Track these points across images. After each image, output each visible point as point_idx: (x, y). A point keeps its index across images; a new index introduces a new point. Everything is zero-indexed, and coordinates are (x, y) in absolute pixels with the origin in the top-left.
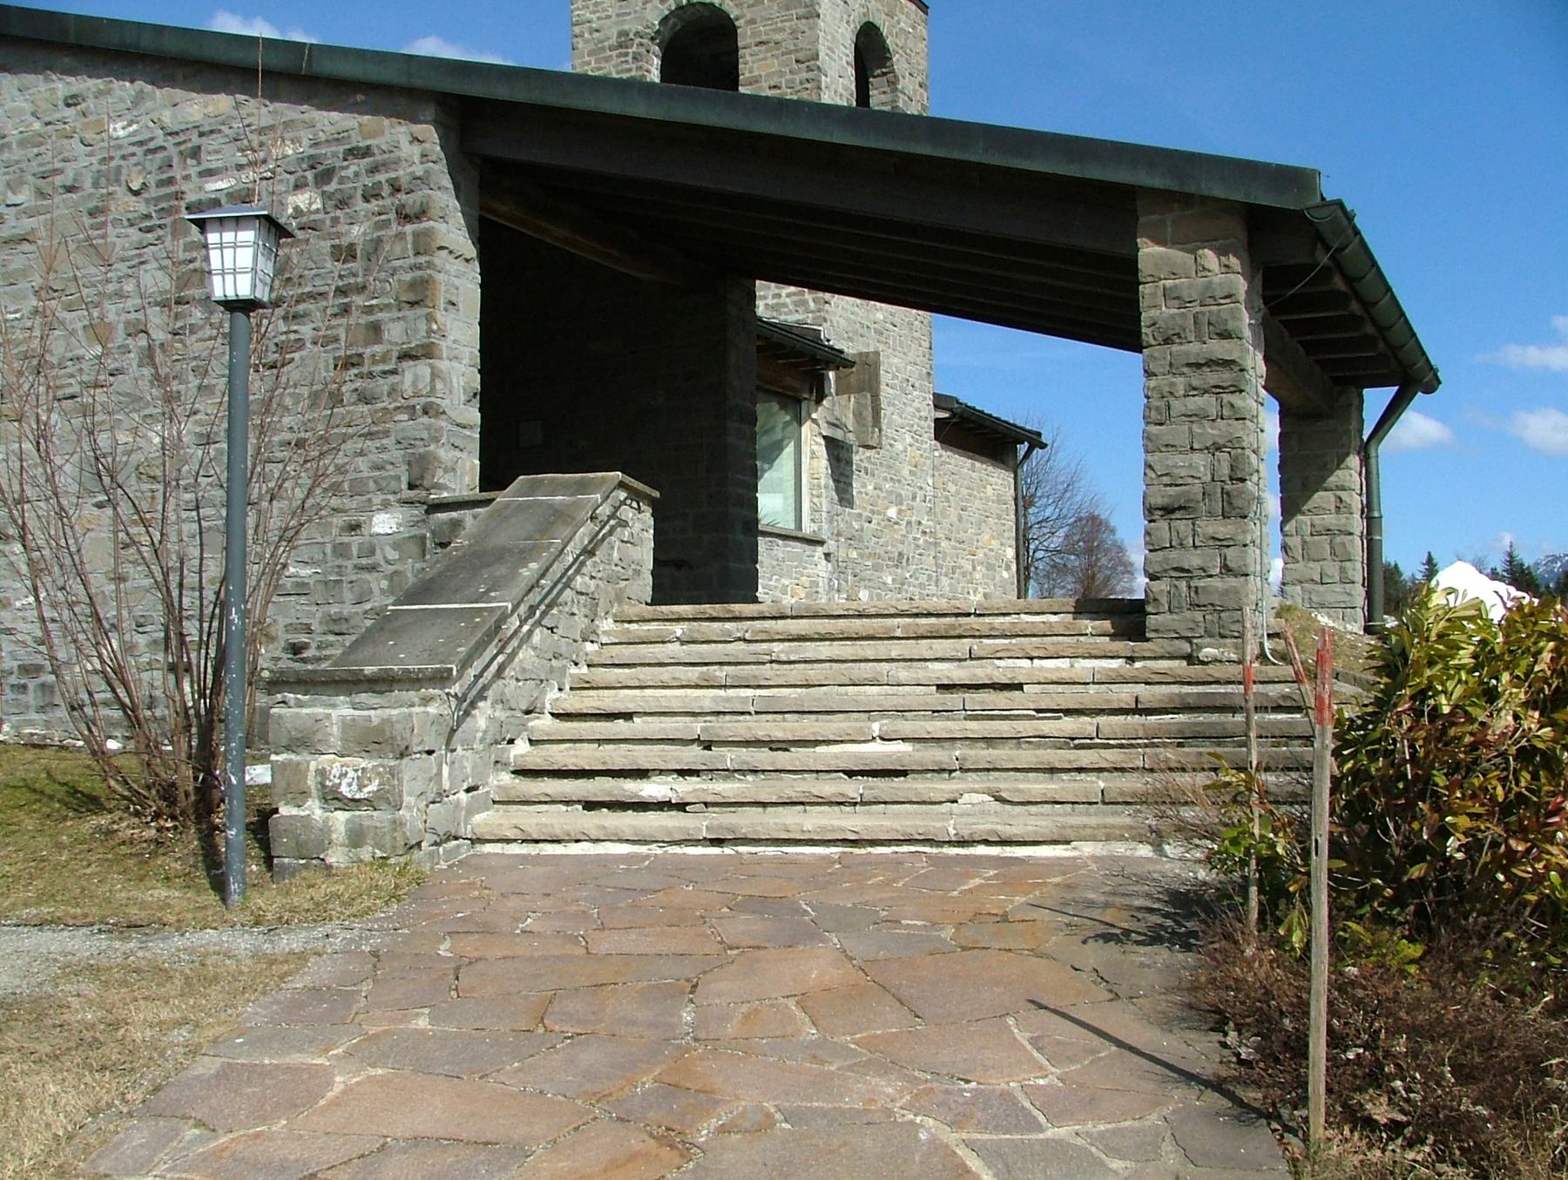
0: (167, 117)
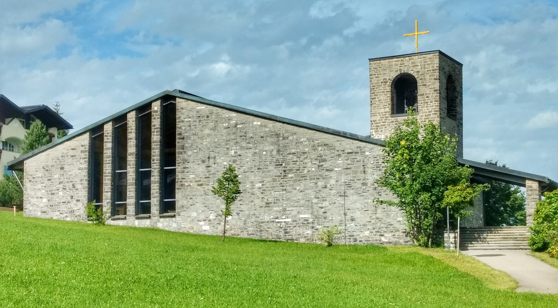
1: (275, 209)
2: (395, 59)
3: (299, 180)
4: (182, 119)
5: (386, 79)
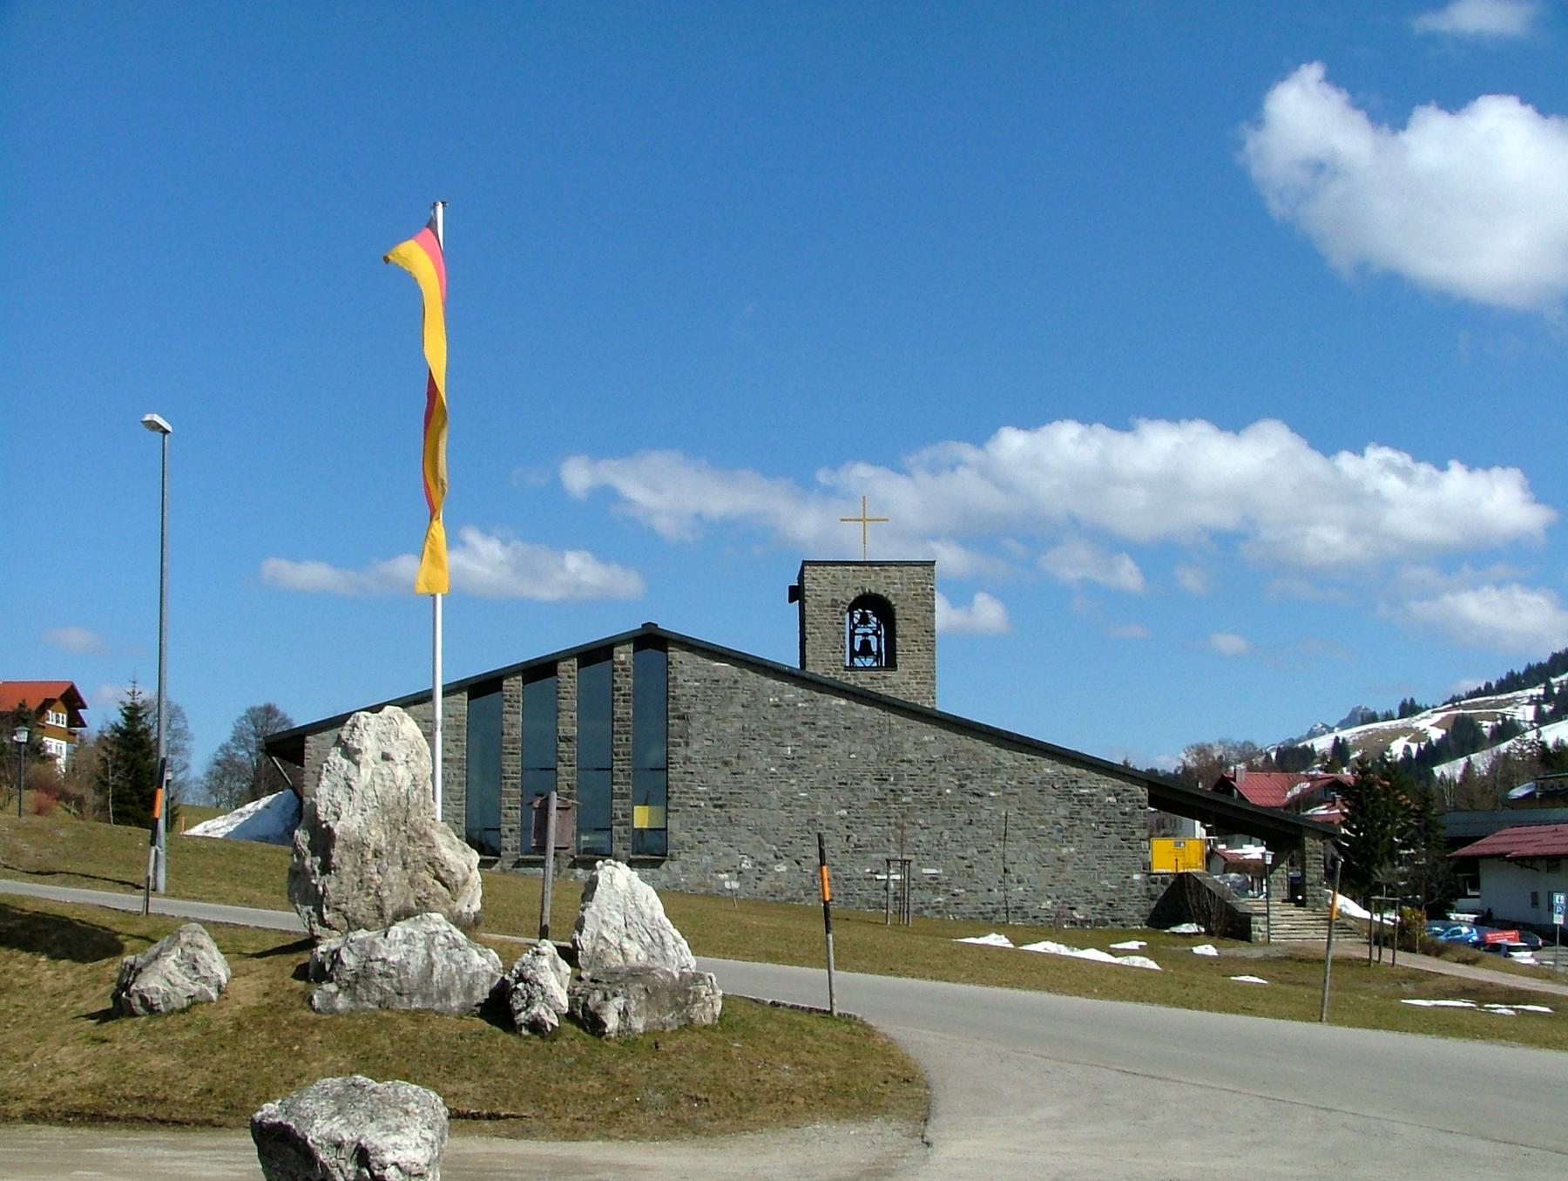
0: (1065, 770)
1: (874, 856)
2: (854, 568)
3: (921, 809)
4: (680, 681)
5: (836, 601)
